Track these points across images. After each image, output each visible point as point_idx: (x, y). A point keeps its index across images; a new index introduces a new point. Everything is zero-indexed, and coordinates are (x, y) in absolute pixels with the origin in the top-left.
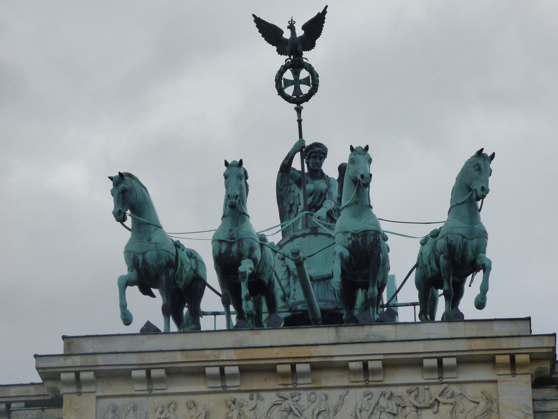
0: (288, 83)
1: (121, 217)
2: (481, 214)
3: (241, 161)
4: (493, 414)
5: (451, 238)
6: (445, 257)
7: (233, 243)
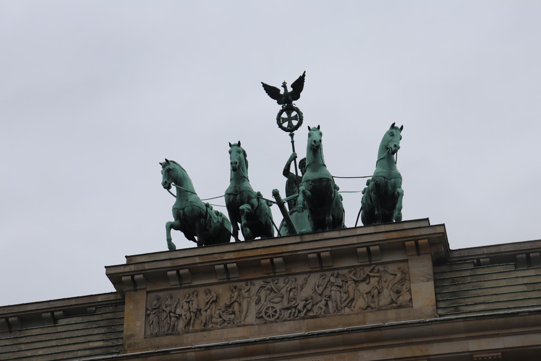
0: (284, 120)
1: (167, 185)
2: (398, 165)
3: (239, 142)
4: (407, 281)
5: (377, 179)
6: (374, 193)
7: (237, 194)
